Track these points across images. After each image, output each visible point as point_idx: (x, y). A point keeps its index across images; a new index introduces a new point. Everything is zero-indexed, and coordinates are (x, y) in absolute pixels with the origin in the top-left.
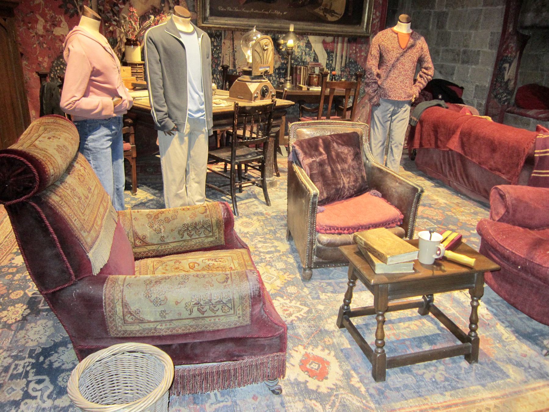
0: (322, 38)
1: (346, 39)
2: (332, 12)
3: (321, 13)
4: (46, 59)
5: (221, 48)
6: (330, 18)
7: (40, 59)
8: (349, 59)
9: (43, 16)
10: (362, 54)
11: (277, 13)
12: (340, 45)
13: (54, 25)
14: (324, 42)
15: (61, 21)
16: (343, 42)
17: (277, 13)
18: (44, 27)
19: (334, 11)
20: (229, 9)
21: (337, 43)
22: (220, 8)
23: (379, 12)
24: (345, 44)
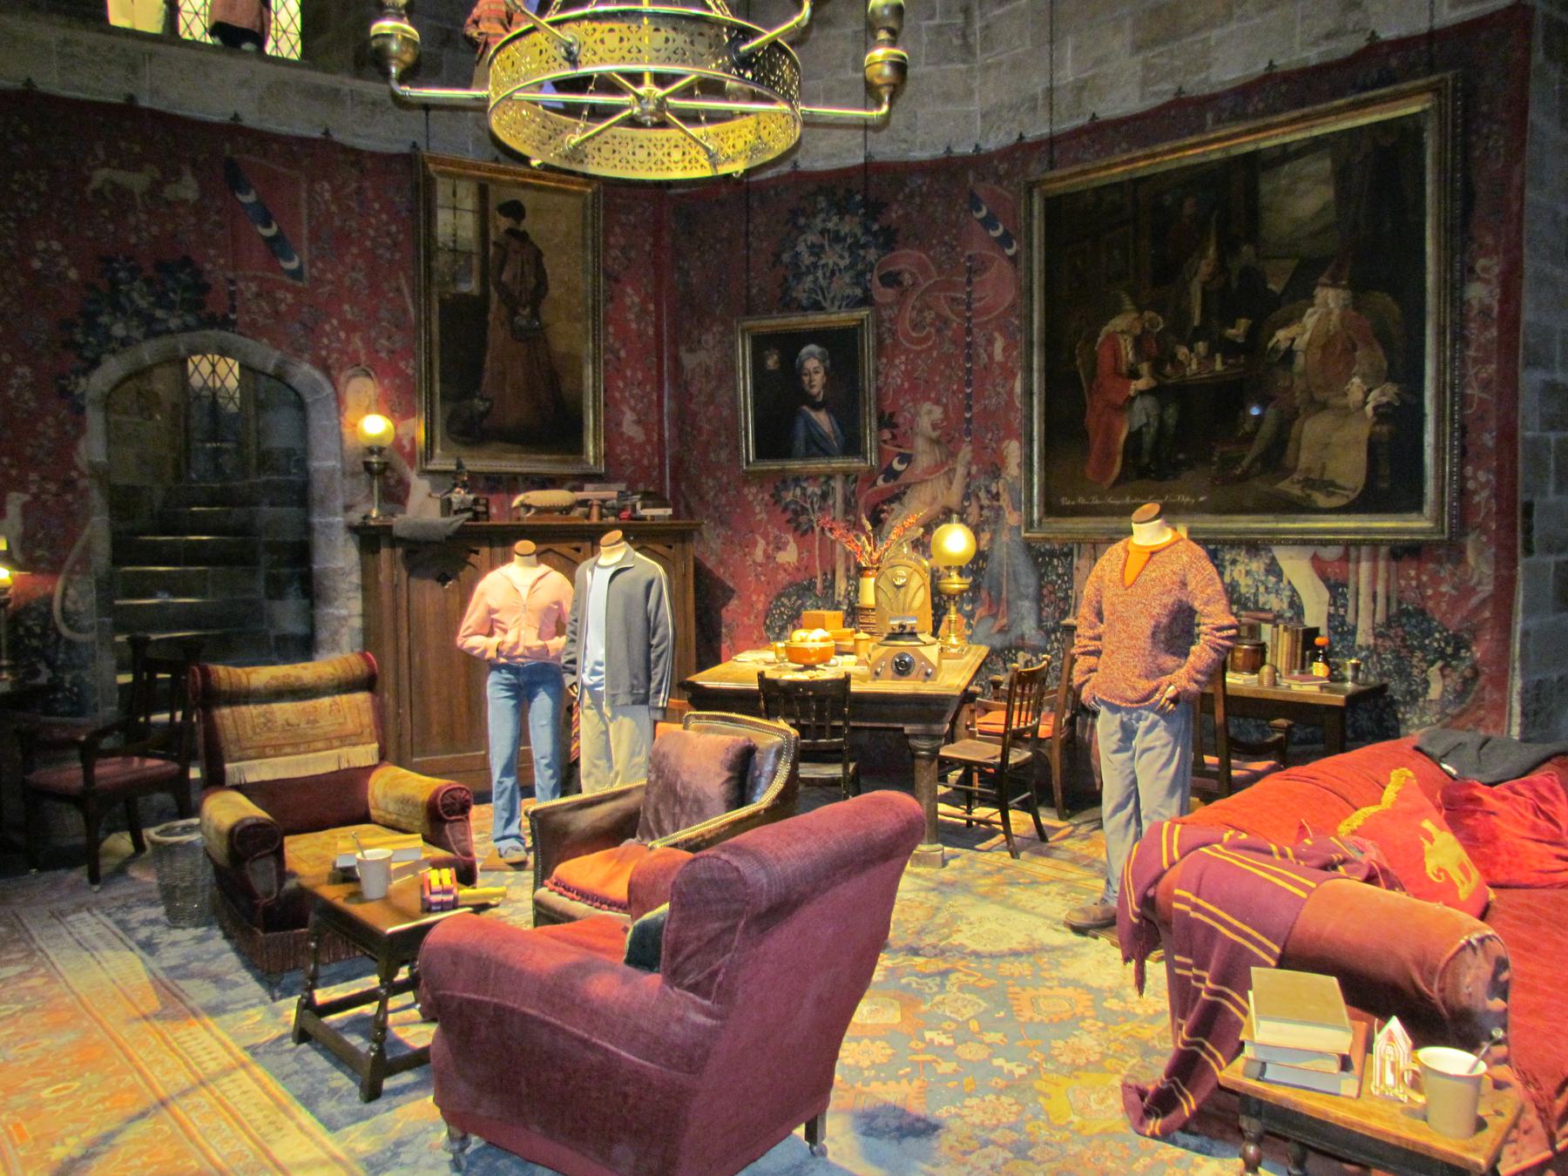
0: (1309, 551)
1: (1384, 550)
2: (1329, 487)
3: (1296, 491)
4: (762, 598)
5: (1071, 580)
6: (1321, 500)
7: (754, 598)
8: (1399, 603)
9: (765, 536)
10: (1444, 588)
11: (1186, 499)
12: (1365, 567)
13: (779, 549)
14: (1316, 561)
15: (787, 543)
16: (1374, 558)
17: (1186, 499)
18: (765, 551)
19: (1332, 484)
20: (1081, 500)
21: (1358, 561)
22: (1065, 501)
23: (1489, 471)
24: (1382, 564)
